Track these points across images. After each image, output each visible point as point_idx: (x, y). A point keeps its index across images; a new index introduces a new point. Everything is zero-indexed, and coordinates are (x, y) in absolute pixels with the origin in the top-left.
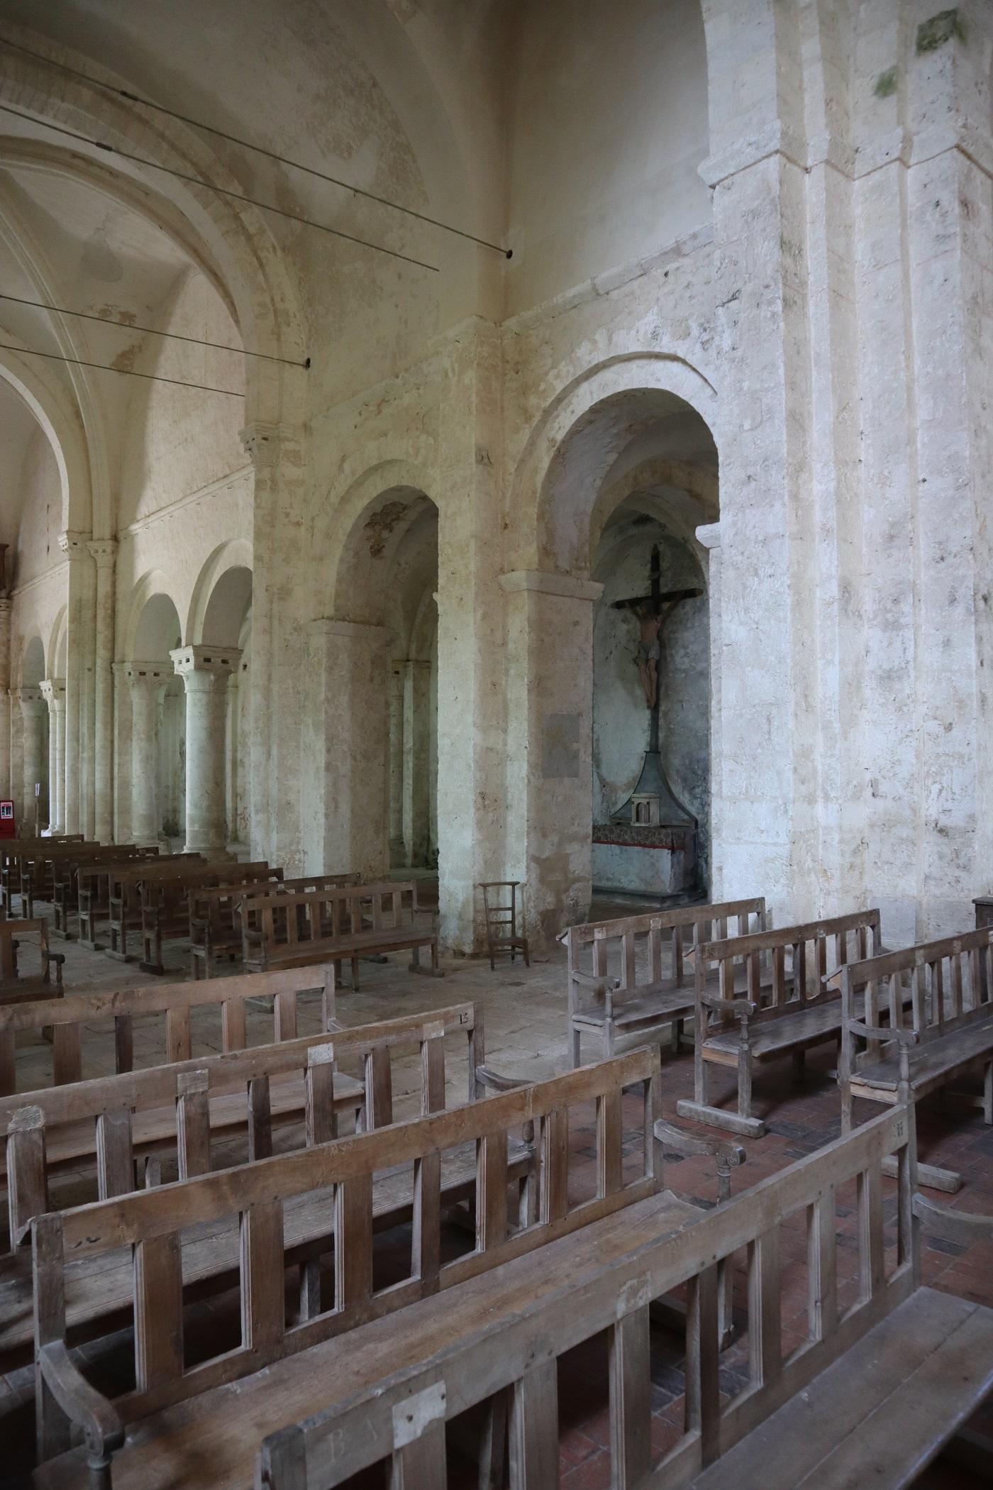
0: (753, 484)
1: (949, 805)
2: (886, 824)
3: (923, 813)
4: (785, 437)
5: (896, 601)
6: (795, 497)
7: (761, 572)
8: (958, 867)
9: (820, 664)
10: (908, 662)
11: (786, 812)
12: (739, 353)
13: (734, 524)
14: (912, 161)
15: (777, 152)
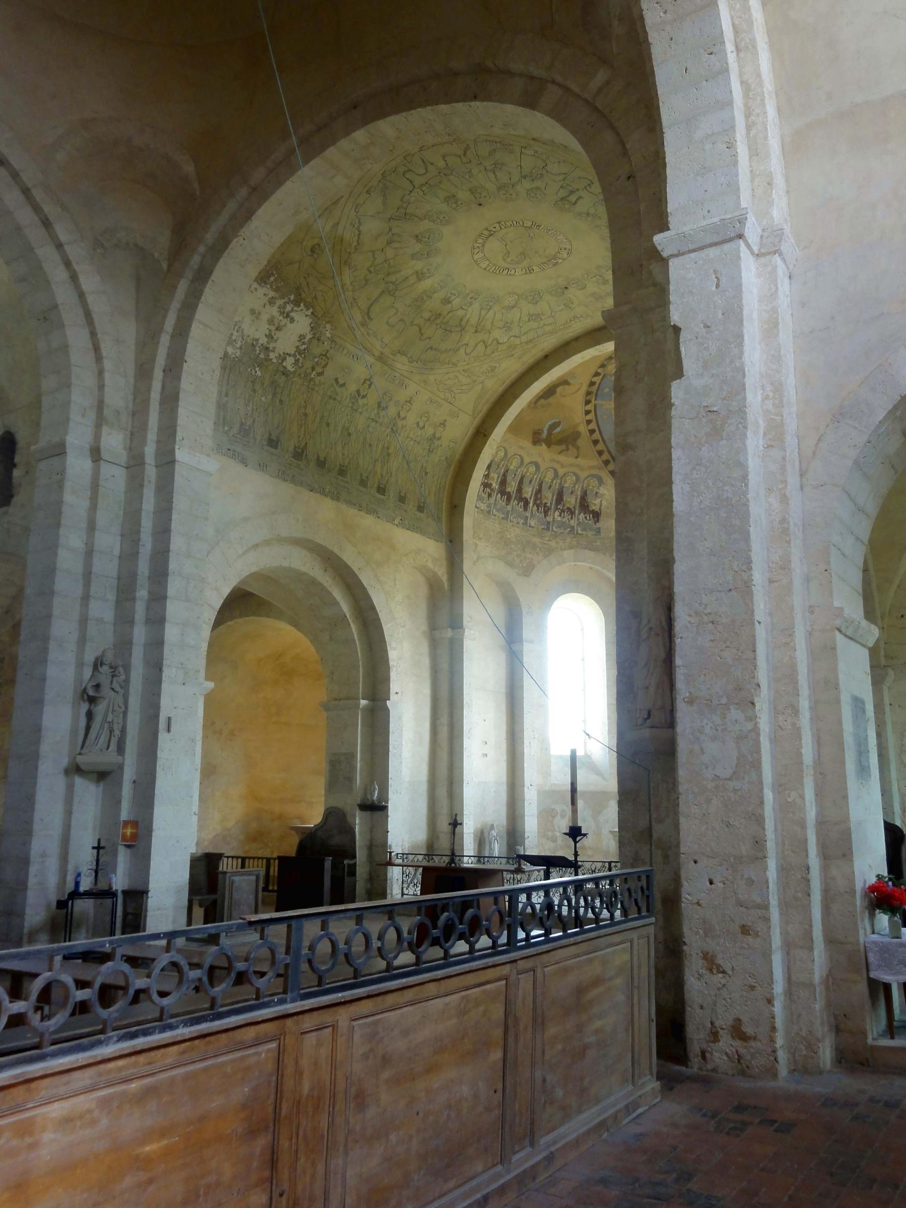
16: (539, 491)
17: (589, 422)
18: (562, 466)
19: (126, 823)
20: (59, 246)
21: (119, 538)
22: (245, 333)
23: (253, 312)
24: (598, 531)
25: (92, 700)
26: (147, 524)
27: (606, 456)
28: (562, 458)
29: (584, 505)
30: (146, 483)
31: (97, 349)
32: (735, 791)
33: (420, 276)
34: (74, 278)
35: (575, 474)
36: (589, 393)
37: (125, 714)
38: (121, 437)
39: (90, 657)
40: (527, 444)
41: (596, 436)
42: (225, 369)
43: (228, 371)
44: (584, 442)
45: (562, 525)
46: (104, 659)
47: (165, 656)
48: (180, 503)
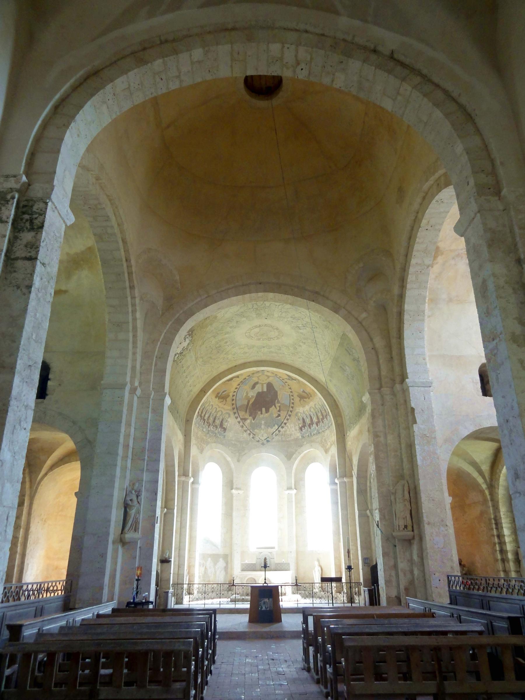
16: (209, 417)
17: (235, 392)
18: (219, 407)
19: (138, 568)
24: (224, 437)
27: (234, 406)
28: (220, 404)
29: (221, 425)
32: (444, 552)
33: (228, 333)
35: (222, 412)
36: (241, 382)
40: (213, 397)
41: (234, 398)
44: (229, 399)
45: (213, 432)
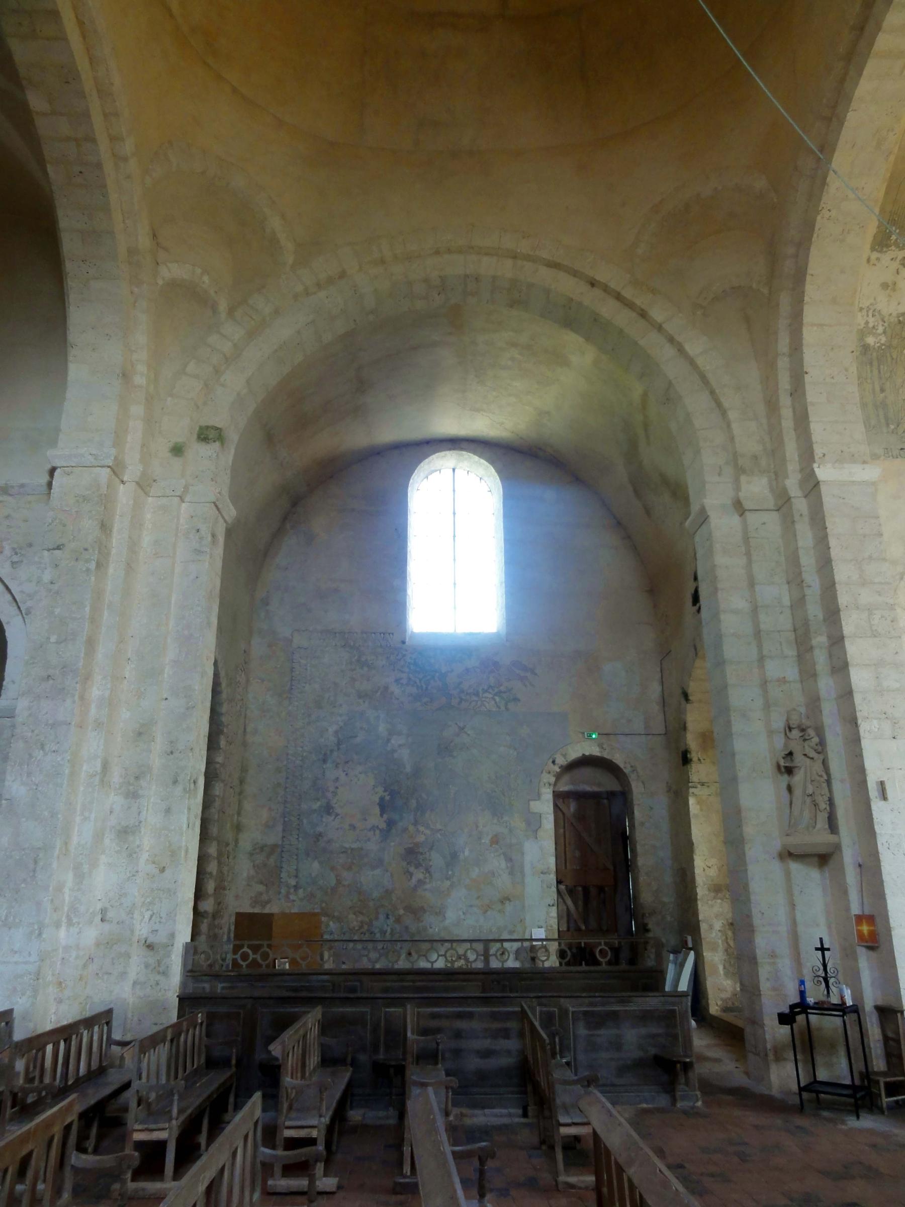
0: (51, 682)
1: (156, 927)
2: (107, 944)
3: (137, 933)
4: (82, 655)
5: (137, 778)
6: (82, 698)
7: (47, 748)
8: (159, 973)
9: (78, 819)
10: (140, 822)
11: (40, 934)
12: (55, 587)
13: (30, 708)
14: (187, 499)
15: (109, 467)
19: (859, 919)
20: (660, 328)
21: (786, 586)
22: (885, 312)
23: (885, 286)
25: (789, 771)
26: (808, 561)
30: (797, 518)
31: (719, 405)
34: (681, 350)
37: (829, 782)
38: (764, 481)
39: (779, 723)
42: (871, 364)
43: (875, 363)
46: (791, 722)
47: (858, 708)
48: (837, 526)
